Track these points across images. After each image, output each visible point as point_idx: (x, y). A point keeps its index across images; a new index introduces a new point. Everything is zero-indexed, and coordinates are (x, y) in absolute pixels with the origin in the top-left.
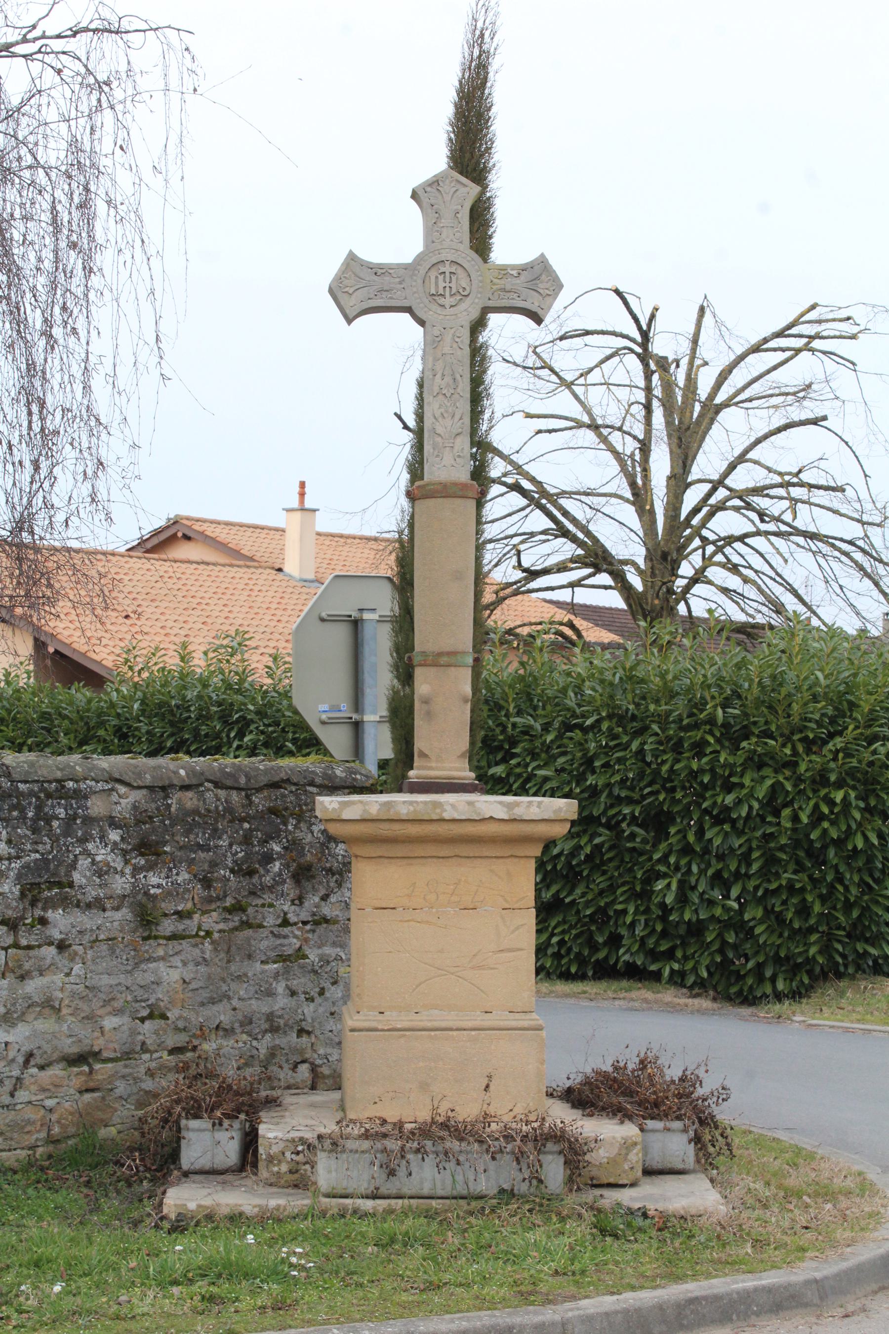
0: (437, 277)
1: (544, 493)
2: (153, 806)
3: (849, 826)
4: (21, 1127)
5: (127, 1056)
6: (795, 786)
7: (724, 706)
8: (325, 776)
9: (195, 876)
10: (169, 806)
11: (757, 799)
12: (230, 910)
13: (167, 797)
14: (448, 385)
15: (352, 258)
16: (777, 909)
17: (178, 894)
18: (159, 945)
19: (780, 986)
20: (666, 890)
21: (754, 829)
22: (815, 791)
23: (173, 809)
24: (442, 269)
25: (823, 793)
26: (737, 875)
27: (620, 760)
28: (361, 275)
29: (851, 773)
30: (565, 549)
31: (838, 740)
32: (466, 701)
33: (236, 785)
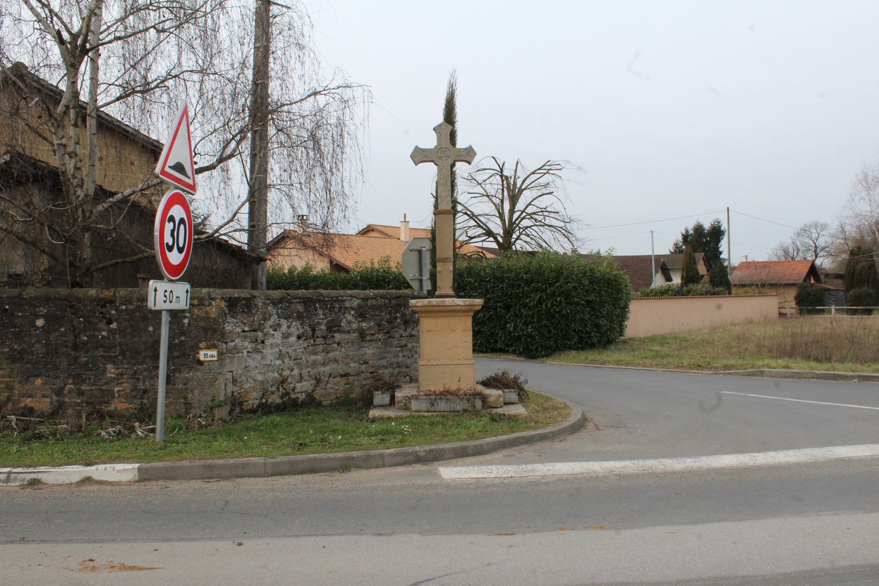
4: (329, 394)
5: (358, 374)
15: (416, 147)
20: (510, 327)
26: (530, 322)
29: (562, 292)
30: (480, 231)
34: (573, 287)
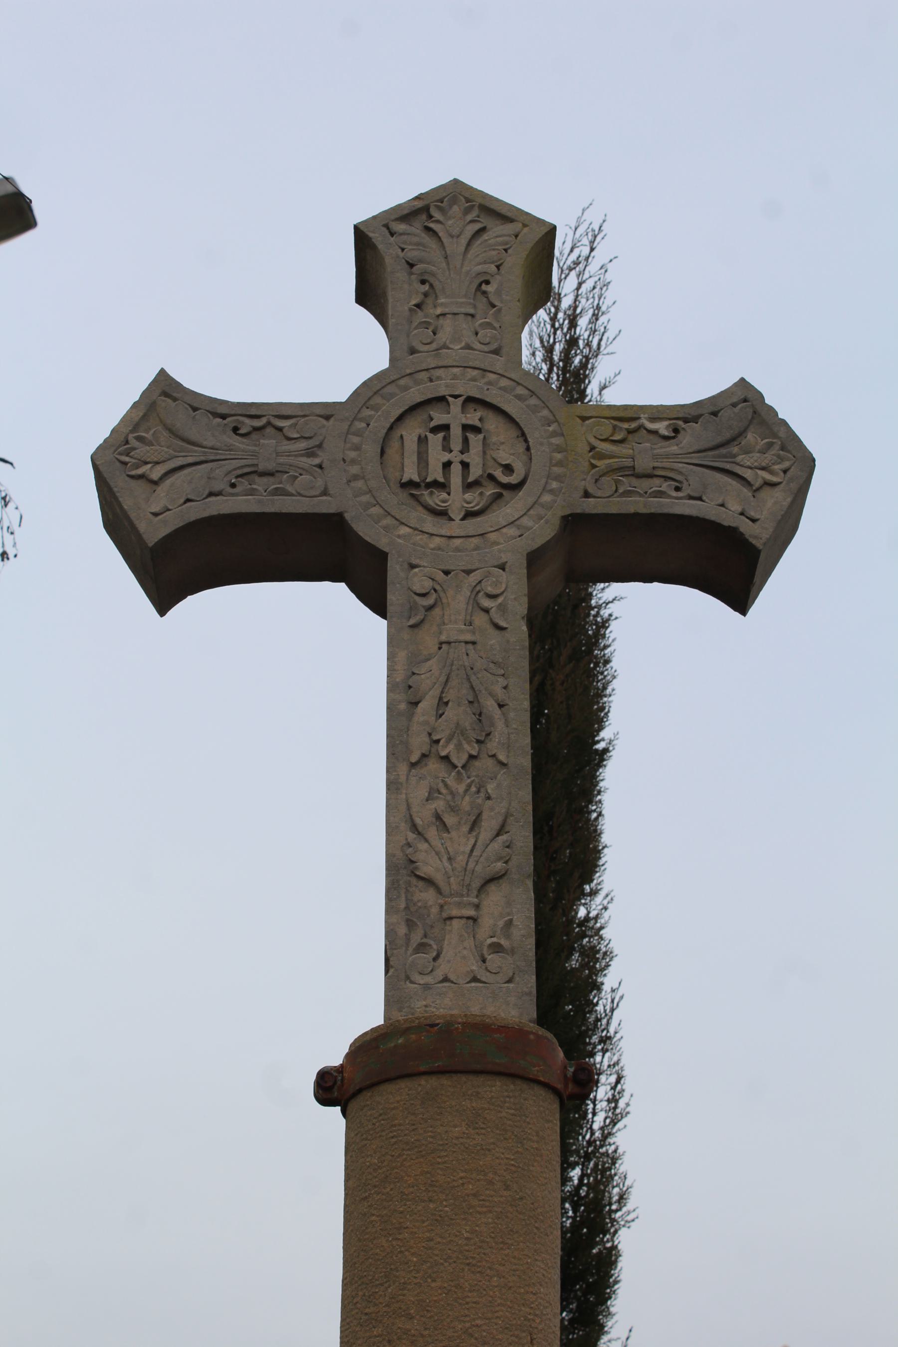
0: (422, 441)
14: (459, 731)
15: (164, 388)
24: (439, 417)
28: (192, 433)
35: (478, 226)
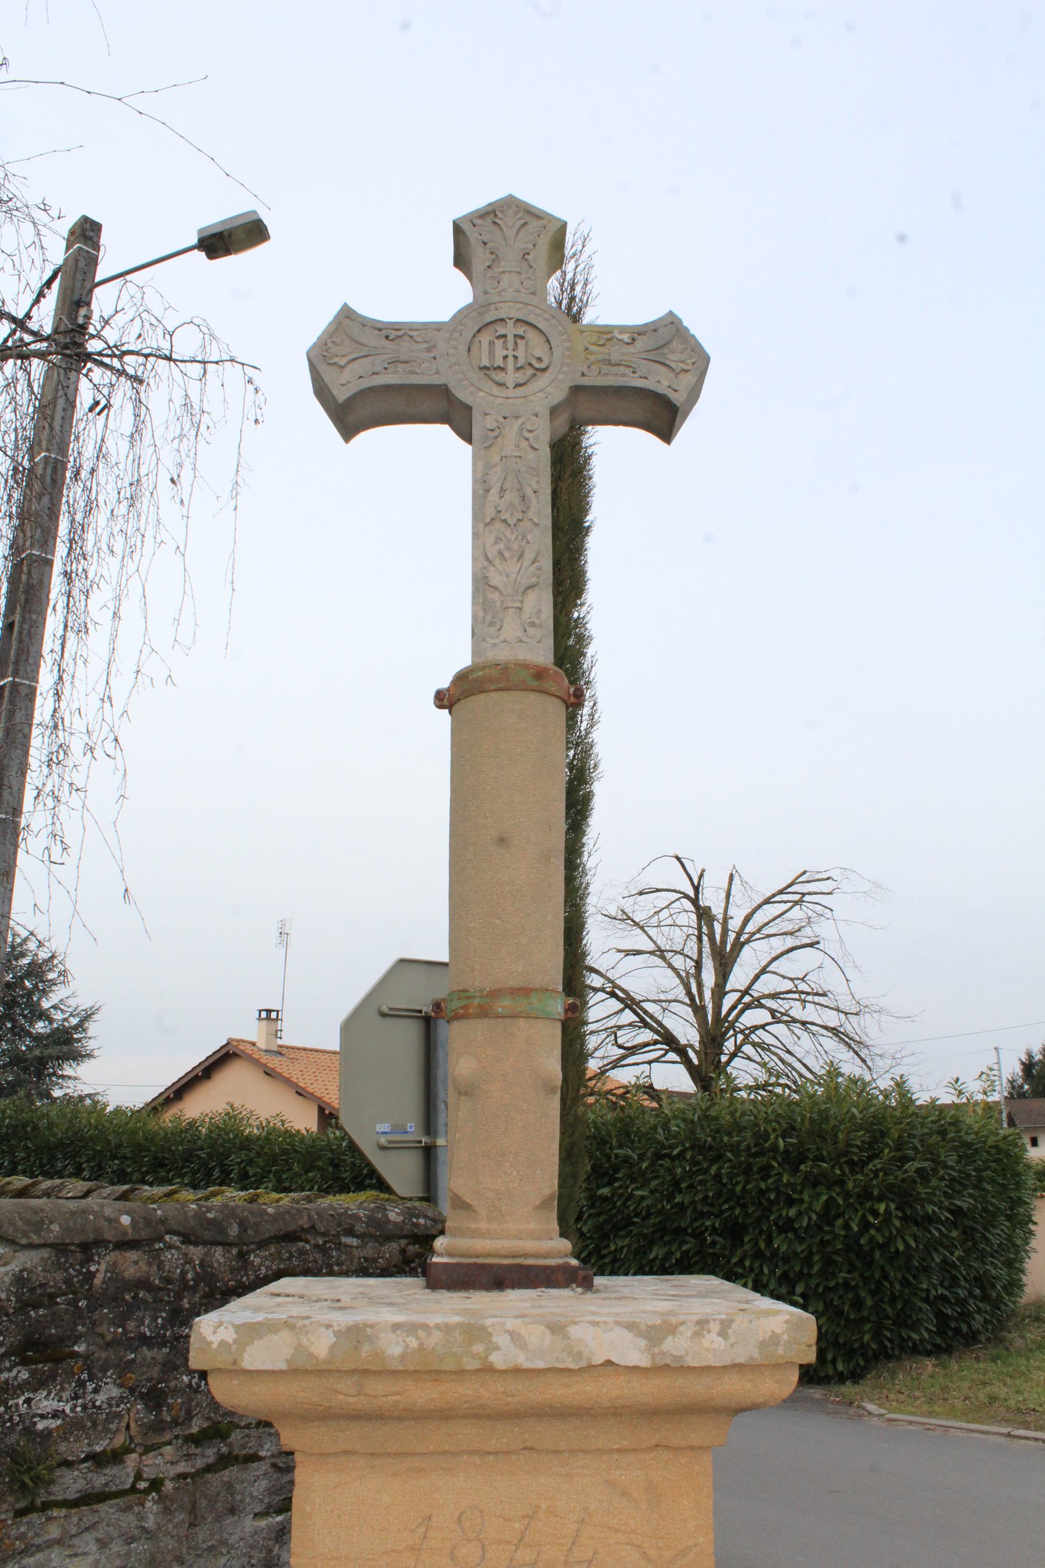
1: (632, 999)
2: (59, 1276)
3: (891, 1232)
6: (845, 1200)
7: (783, 1138)
8: (372, 1221)
9: (132, 1391)
10: (92, 1275)
11: (815, 1212)
12: (195, 1440)
13: (89, 1260)
14: (511, 506)
15: (347, 314)
16: (835, 1303)
17: (95, 1424)
18: (49, 1519)
19: (840, 1367)
21: (812, 1237)
22: (861, 1204)
23: (97, 1281)
24: (501, 331)
25: (868, 1205)
26: (801, 1275)
27: (701, 1182)
28: (363, 340)
29: (890, 1187)
30: (647, 1036)
31: (877, 1161)
32: (552, 1091)
33: (219, 1239)
34: (919, 1171)
35: (523, 222)
